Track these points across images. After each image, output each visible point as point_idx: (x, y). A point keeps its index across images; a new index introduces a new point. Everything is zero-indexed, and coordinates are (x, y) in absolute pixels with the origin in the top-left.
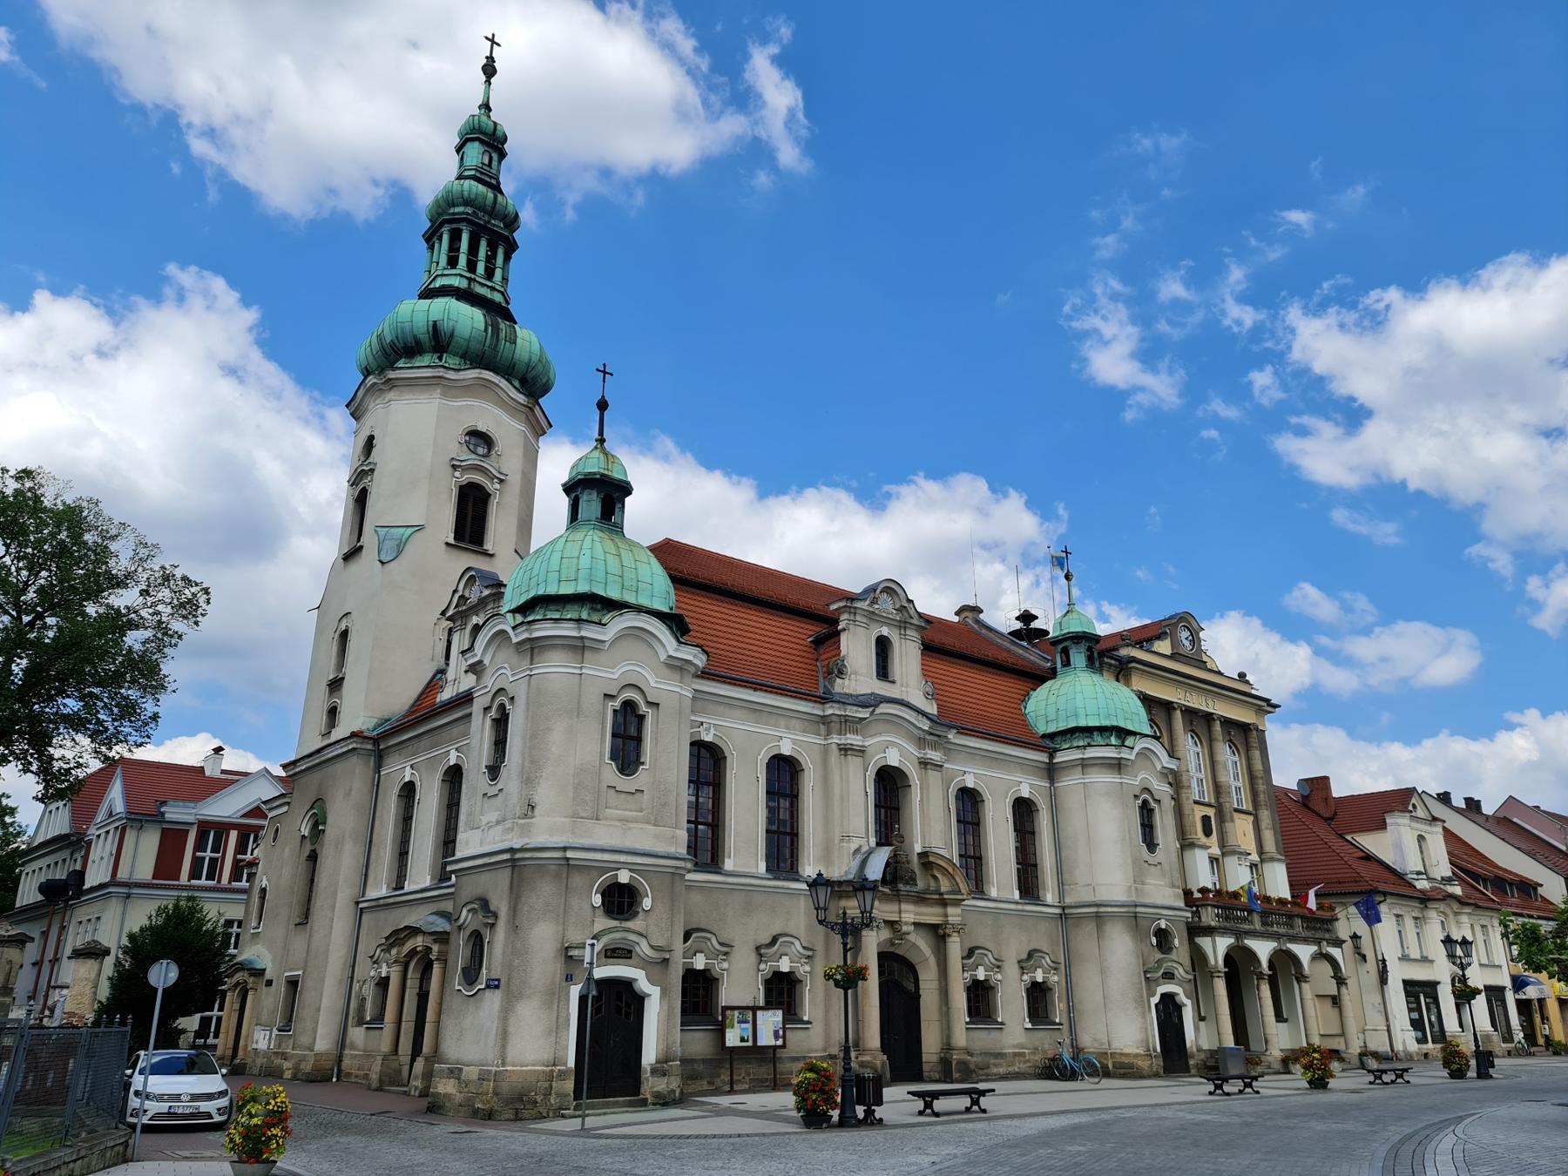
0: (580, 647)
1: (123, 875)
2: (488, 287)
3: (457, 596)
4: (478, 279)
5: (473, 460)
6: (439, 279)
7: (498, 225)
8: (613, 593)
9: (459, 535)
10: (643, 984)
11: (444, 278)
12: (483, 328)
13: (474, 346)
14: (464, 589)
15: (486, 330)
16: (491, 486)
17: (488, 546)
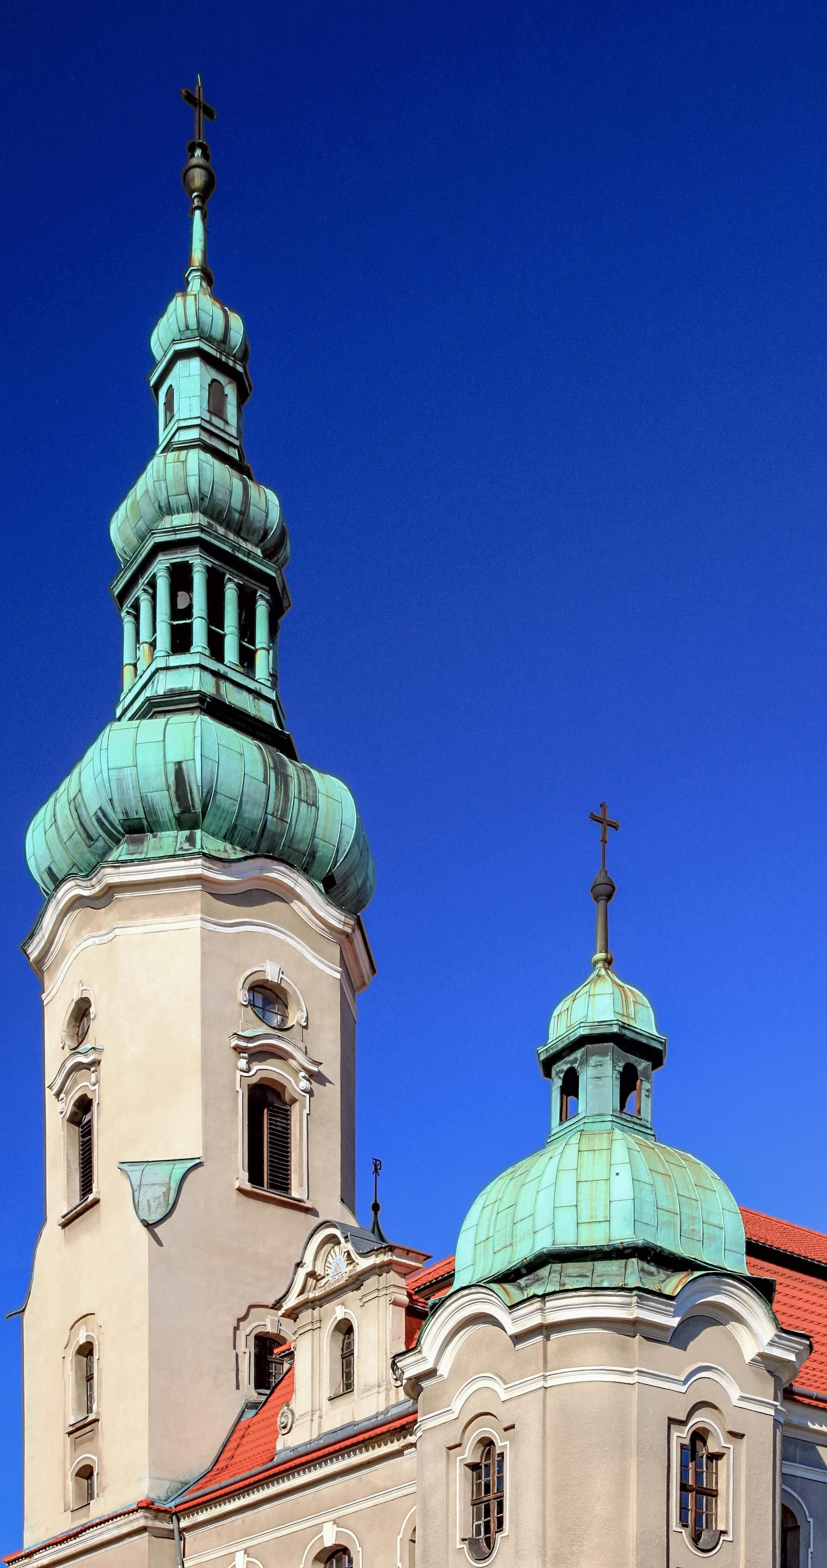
2: (250, 691)
3: (302, 1273)
4: (232, 675)
6: (161, 676)
11: (170, 673)
12: (261, 777)
14: (315, 1260)
15: (265, 780)
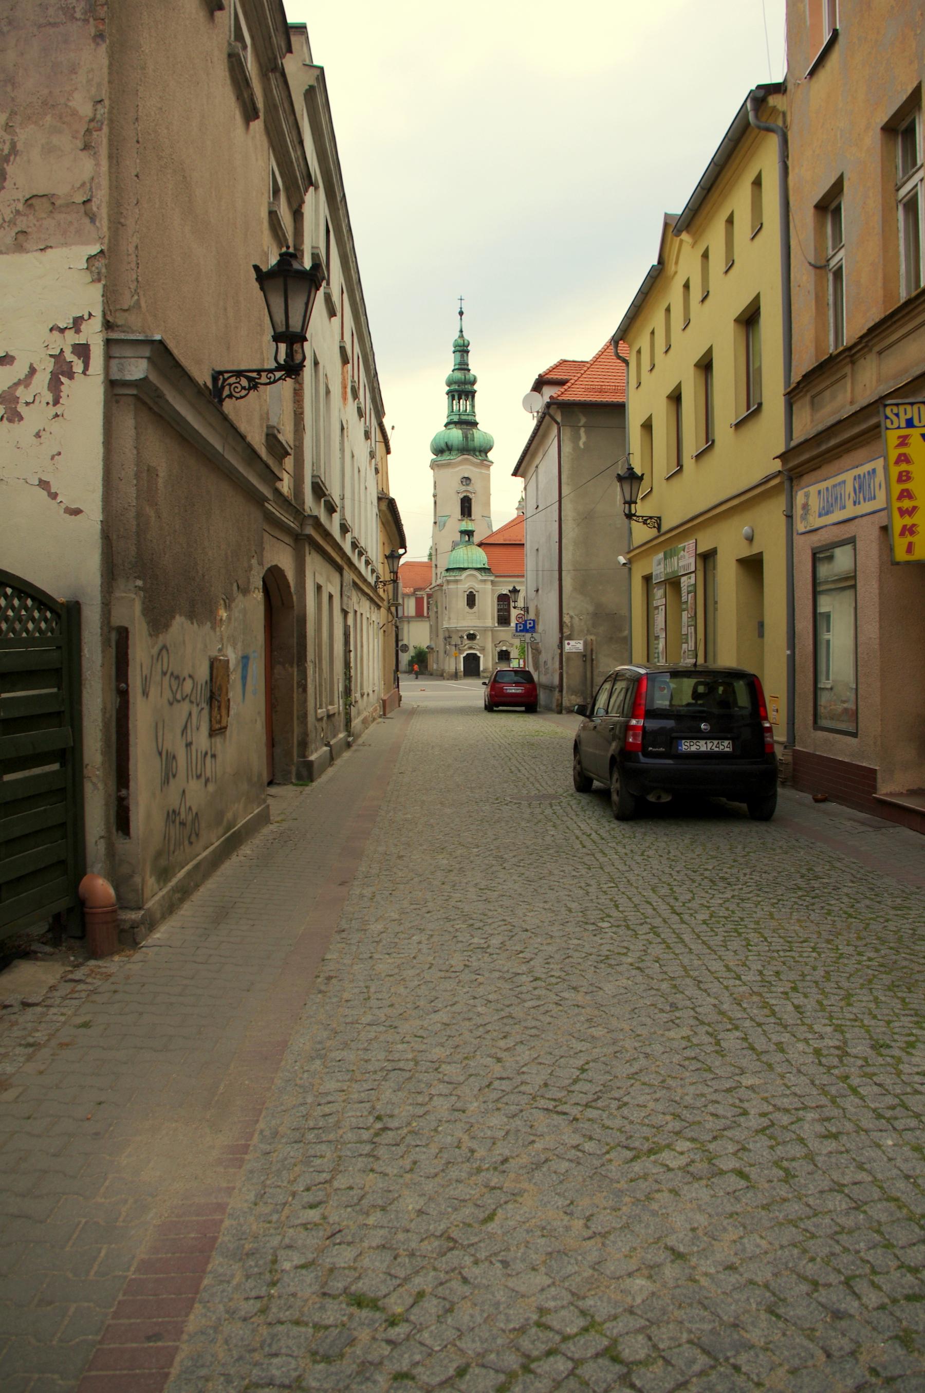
0: (456, 581)
1: (406, 614)
5: (464, 488)
7: (468, 387)
8: (466, 566)
9: (463, 513)
10: (479, 654)
13: (461, 447)
16: (471, 496)
17: (473, 517)
